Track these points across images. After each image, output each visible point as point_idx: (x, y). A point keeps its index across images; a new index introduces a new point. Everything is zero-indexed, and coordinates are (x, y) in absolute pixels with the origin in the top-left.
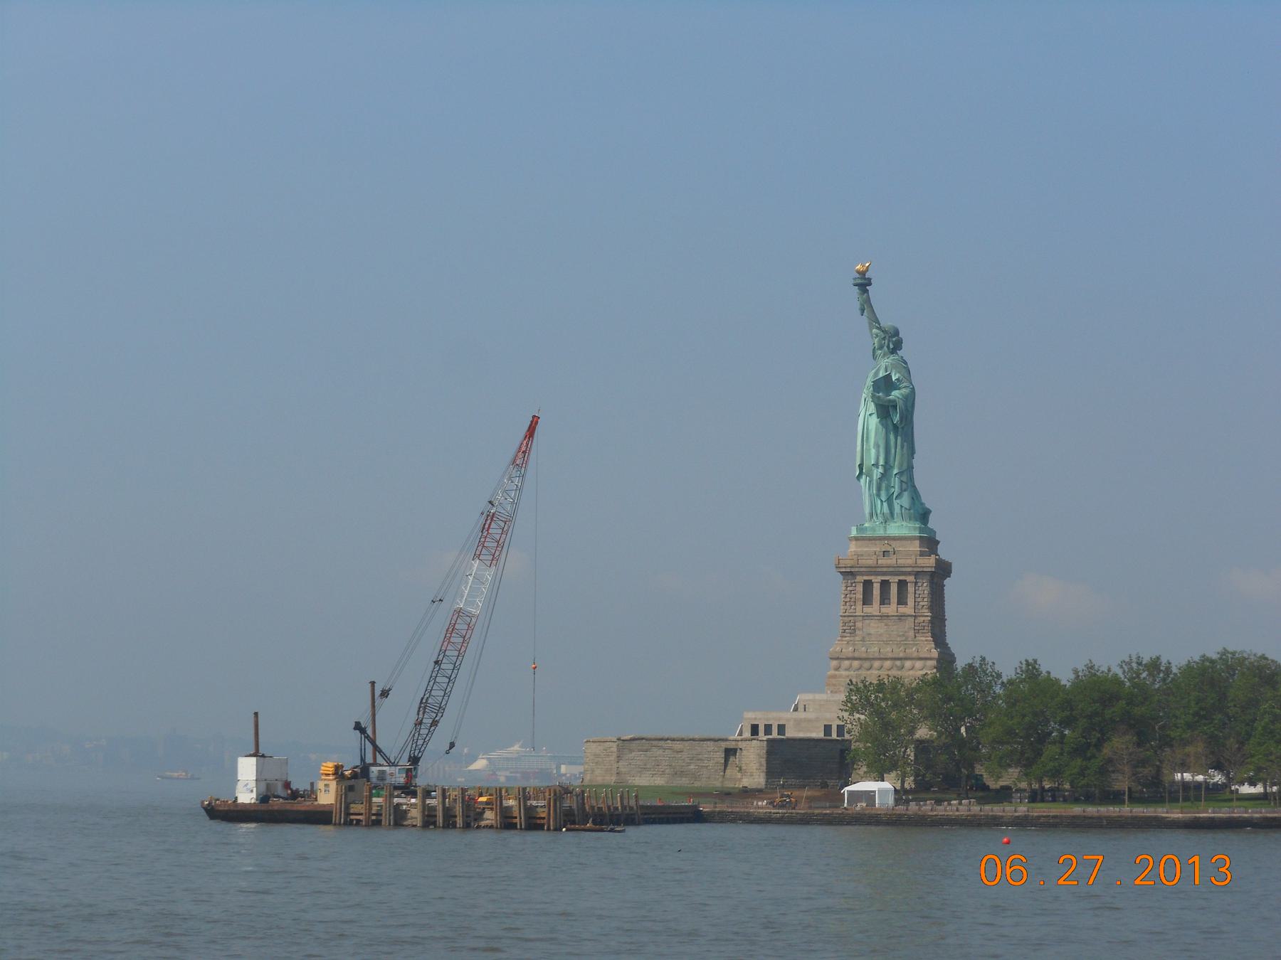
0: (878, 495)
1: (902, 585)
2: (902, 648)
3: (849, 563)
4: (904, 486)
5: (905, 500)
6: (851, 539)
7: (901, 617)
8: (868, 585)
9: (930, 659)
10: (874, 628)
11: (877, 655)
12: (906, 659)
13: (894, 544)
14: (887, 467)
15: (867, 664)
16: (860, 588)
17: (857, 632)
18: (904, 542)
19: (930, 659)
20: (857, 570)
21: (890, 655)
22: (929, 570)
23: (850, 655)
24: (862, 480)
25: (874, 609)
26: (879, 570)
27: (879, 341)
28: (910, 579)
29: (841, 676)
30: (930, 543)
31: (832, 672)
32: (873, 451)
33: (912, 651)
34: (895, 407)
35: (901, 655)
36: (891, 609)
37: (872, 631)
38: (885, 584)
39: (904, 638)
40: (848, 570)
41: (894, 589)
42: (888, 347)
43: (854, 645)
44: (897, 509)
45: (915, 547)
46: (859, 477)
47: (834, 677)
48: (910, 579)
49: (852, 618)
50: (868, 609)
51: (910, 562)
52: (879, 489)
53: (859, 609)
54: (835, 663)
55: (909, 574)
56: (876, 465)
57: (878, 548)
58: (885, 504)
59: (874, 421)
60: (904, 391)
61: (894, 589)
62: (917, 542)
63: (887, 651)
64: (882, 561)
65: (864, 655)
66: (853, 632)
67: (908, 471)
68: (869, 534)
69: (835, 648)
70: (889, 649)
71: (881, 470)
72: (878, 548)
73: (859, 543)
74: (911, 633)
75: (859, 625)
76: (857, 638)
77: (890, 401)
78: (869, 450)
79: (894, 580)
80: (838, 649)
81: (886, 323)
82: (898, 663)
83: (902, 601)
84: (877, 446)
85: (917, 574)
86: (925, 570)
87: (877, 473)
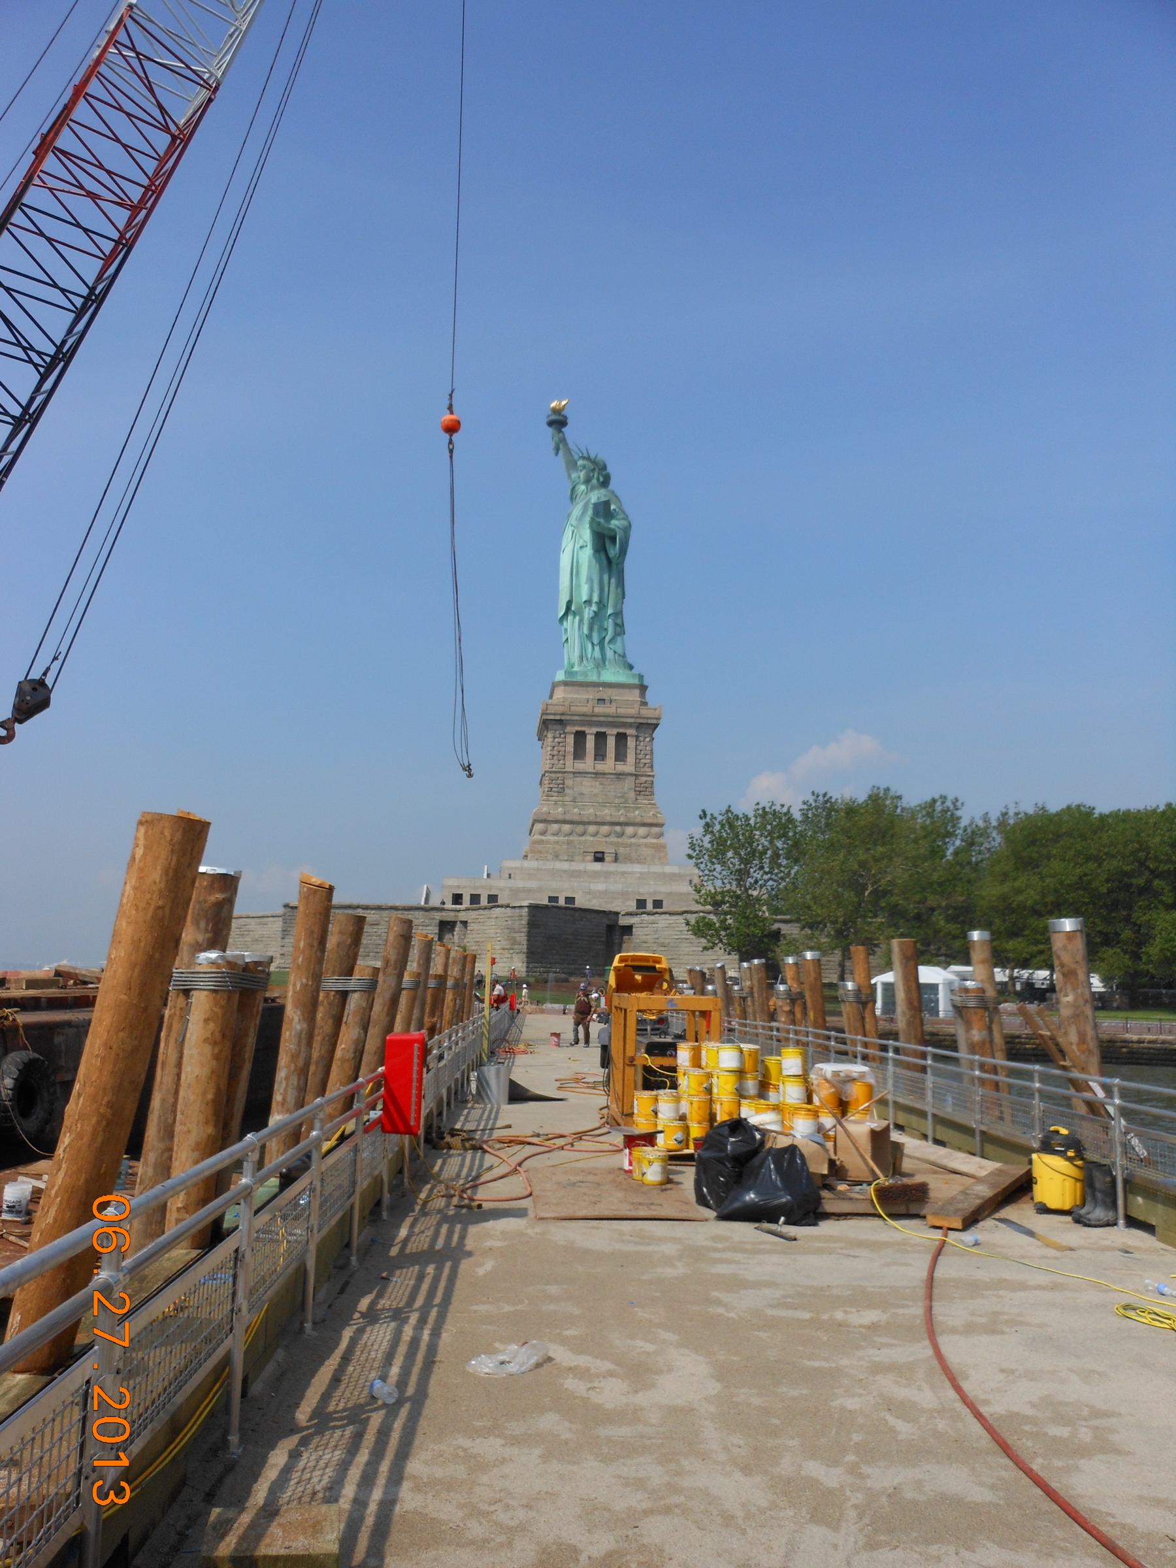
0: (589, 637)
1: (621, 738)
3: (560, 709)
7: (620, 776)
8: (580, 736)
10: (588, 786)
12: (627, 824)
14: (602, 605)
15: (580, 828)
16: (570, 740)
17: (567, 791)
18: (622, 691)
20: (568, 718)
21: (608, 819)
23: (560, 817)
25: (588, 763)
26: (595, 719)
29: (548, 842)
35: (622, 819)
36: (609, 764)
37: (585, 790)
38: (601, 737)
40: (558, 718)
41: (611, 742)
42: (598, 479)
43: (564, 806)
44: (609, 654)
46: (562, 619)
47: (541, 842)
48: (630, 731)
49: (560, 775)
50: (580, 766)
51: (632, 711)
52: (591, 629)
53: (570, 764)
55: (630, 725)
56: (588, 602)
57: (591, 695)
58: (597, 648)
59: (588, 551)
61: (611, 742)
63: (607, 813)
64: (599, 709)
65: (577, 818)
66: (561, 792)
67: (618, 614)
68: (580, 678)
71: (594, 608)
74: (632, 795)
75: (569, 782)
76: (567, 798)
78: (579, 586)
82: (618, 828)
83: (620, 756)
86: (649, 721)
87: (588, 613)
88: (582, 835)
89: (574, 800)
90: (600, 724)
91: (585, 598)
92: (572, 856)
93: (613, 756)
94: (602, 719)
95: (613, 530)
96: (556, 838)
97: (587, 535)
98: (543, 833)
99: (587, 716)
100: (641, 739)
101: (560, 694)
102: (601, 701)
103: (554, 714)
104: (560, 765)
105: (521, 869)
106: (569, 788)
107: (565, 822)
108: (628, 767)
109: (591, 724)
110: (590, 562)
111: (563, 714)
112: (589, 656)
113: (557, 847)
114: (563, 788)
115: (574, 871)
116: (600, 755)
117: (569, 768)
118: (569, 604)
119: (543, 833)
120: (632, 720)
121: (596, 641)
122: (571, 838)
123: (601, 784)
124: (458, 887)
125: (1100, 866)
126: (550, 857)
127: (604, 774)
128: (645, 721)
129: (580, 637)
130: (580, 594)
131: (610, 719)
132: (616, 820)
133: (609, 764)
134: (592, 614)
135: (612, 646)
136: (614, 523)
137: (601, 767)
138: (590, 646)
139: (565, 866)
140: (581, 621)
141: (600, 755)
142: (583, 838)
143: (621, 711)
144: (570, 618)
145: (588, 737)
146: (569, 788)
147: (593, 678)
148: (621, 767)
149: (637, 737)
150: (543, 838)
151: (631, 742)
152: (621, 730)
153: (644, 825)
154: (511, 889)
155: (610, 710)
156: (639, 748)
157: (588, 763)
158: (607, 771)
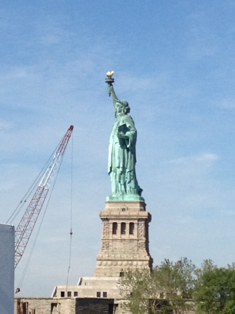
0: (120, 182)
1: (132, 225)
2: (132, 255)
3: (106, 214)
4: (132, 178)
5: (132, 184)
6: (106, 203)
7: (131, 240)
8: (115, 225)
9: (146, 260)
10: (118, 245)
11: (119, 259)
12: (133, 260)
13: (127, 205)
14: (124, 168)
15: (115, 263)
16: (111, 226)
17: (110, 247)
18: (132, 204)
19: (146, 260)
20: (110, 217)
21: (126, 259)
22: (145, 218)
23: (107, 259)
24: (111, 174)
25: (118, 235)
26: (120, 217)
27: (119, 108)
28: (135, 222)
29: (102, 269)
30: (143, 205)
31: (98, 267)
32: (117, 161)
33: (137, 257)
34: (128, 140)
35: (132, 259)
36: (127, 236)
37: (117, 247)
38: (123, 225)
39: (132, 251)
40: (105, 217)
41: (128, 227)
42: (124, 111)
43: (108, 254)
44: (128, 189)
45: (138, 206)
46: (109, 173)
47: (99, 269)
48: (135, 222)
49: (106, 241)
50: (115, 236)
51: (135, 213)
52: (120, 179)
53: (111, 236)
54: (99, 262)
55: (135, 219)
56: (119, 167)
57: (120, 207)
58: (123, 186)
59: (118, 145)
60: (133, 132)
61: (128, 227)
62: (139, 205)
63: (125, 256)
64: (122, 213)
65: (113, 259)
66: (108, 247)
67: (133, 171)
68: (115, 200)
69: (100, 254)
70: (125, 256)
71: (121, 169)
72: (120, 207)
73: (111, 204)
74: (136, 248)
75: (111, 244)
76: (110, 250)
77: (126, 137)
78: (115, 160)
79: (128, 222)
80: (101, 255)
81: (123, 100)
82: (130, 262)
83: (131, 233)
84: (119, 158)
85: (139, 220)
86: (143, 217)
87: (119, 171)
88: (115, 265)
89: (113, 251)
90: (123, 219)
91: (117, 166)
92: (112, 273)
93: (129, 232)
94: (123, 217)
95: (127, 137)
96: (105, 267)
97: (117, 140)
98: (100, 265)
99: (117, 216)
100: (140, 224)
101: (107, 206)
102: (123, 210)
103: (104, 216)
104: (107, 237)
105: (90, 281)
106: (111, 246)
107: (109, 260)
108: (134, 237)
109: (119, 219)
110: (119, 149)
111: (107, 216)
112: (120, 189)
113: (105, 270)
114: (108, 246)
115: (110, 281)
116: (123, 232)
117: (111, 238)
118: (111, 168)
119: (100, 265)
120: (135, 217)
121: (122, 183)
122: (111, 267)
123: (124, 244)
124: (63, 289)
125: (216, 279)
126: (103, 275)
127: (125, 240)
128: (140, 218)
129: (116, 182)
130: (115, 164)
131: (127, 217)
132: (129, 259)
133: (127, 236)
134: (120, 172)
135: (129, 184)
136: (128, 133)
137: (124, 237)
138: (120, 185)
139: (107, 279)
140: (116, 175)
141: (123, 232)
142: (116, 267)
143: (131, 214)
144: (112, 172)
145: (118, 225)
146: (111, 246)
147: (121, 199)
148: (132, 237)
149: (138, 224)
150: (100, 267)
151: (136, 226)
152: (132, 221)
153: (140, 260)
154: (83, 290)
155: (126, 213)
156: (139, 228)
157: (118, 235)
158: (126, 239)
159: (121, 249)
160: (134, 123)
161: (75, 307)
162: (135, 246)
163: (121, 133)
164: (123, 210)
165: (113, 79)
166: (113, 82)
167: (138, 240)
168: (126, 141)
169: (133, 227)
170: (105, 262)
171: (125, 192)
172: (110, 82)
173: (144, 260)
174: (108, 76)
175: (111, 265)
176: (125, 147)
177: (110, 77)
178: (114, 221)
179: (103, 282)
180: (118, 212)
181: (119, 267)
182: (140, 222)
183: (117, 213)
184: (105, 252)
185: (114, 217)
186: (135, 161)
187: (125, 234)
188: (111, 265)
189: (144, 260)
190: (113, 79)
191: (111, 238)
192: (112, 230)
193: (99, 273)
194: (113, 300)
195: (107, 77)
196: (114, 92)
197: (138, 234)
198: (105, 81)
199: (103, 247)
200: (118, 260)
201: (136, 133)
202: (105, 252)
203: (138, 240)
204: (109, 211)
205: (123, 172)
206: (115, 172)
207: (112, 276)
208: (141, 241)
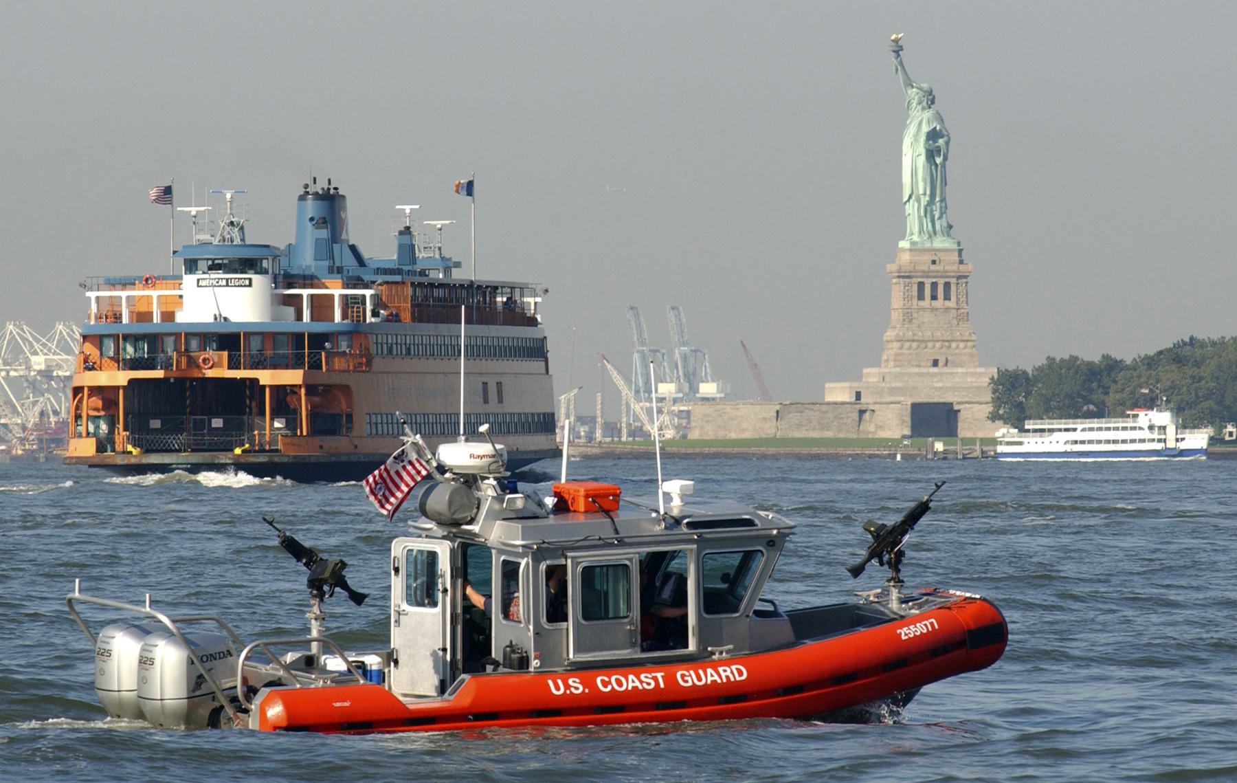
1: (947, 285)
7: (947, 309)
10: (927, 317)
11: (931, 338)
12: (953, 341)
14: (933, 195)
15: (923, 345)
16: (915, 287)
17: (914, 321)
21: (941, 338)
23: (911, 338)
25: (927, 302)
27: (920, 98)
29: (904, 354)
32: (921, 185)
35: (949, 338)
36: (939, 303)
37: (925, 320)
44: (938, 227)
45: (955, 257)
50: (922, 303)
54: (898, 344)
55: (953, 277)
65: (921, 338)
71: (927, 198)
75: (915, 315)
76: (915, 325)
79: (941, 282)
82: (947, 344)
83: (947, 297)
84: (924, 180)
87: (925, 200)
89: (919, 326)
102: (934, 262)
107: (914, 341)
108: (952, 304)
109: (927, 277)
112: (925, 229)
117: (915, 307)
120: (953, 274)
127: (937, 309)
134: (926, 203)
136: (941, 142)
137: (935, 304)
139: (916, 370)
145: (926, 285)
147: (928, 245)
148: (947, 303)
150: (901, 351)
151: (953, 288)
152: (947, 280)
154: (889, 388)
159: (932, 323)
160: (942, 120)
161: (910, 416)
162: (953, 318)
163: (931, 142)
164: (934, 262)
165: (901, 47)
166: (902, 50)
167: (958, 309)
168: (935, 153)
169: (950, 288)
170: (907, 344)
171: (933, 235)
172: (898, 49)
173: (968, 341)
174: (893, 41)
175: (942, 347)
176: (932, 162)
177: (896, 41)
178: (920, 280)
179: (910, 375)
180: (927, 265)
181: (930, 351)
182: (960, 281)
183: (925, 268)
184: (908, 329)
185: (919, 274)
186: (944, 182)
187: (924, 299)
188: (942, 347)
189: (968, 341)
190: (901, 47)
191: (916, 307)
192: (916, 294)
193: (900, 361)
194: (952, 404)
195: (892, 43)
196: (903, 68)
197: (958, 299)
198: (889, 48)
199: (904, 320)
200: (928, 341)
201: (949, 139)
202: (908, 329)
203: (958, 309)
204: (912, 265)
205: (931, 202)
206: (918, 201)
207: (920, 366)
208: (962, 311)
